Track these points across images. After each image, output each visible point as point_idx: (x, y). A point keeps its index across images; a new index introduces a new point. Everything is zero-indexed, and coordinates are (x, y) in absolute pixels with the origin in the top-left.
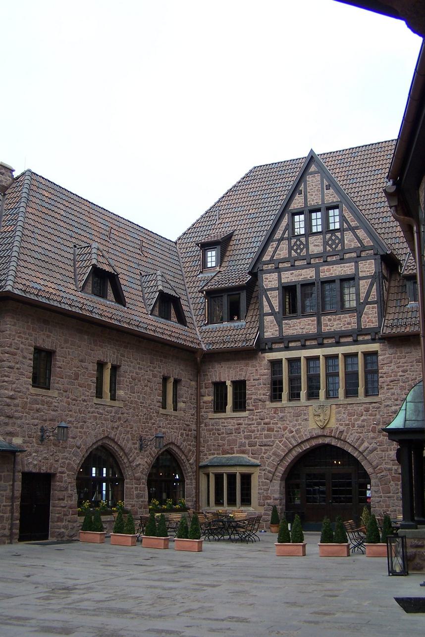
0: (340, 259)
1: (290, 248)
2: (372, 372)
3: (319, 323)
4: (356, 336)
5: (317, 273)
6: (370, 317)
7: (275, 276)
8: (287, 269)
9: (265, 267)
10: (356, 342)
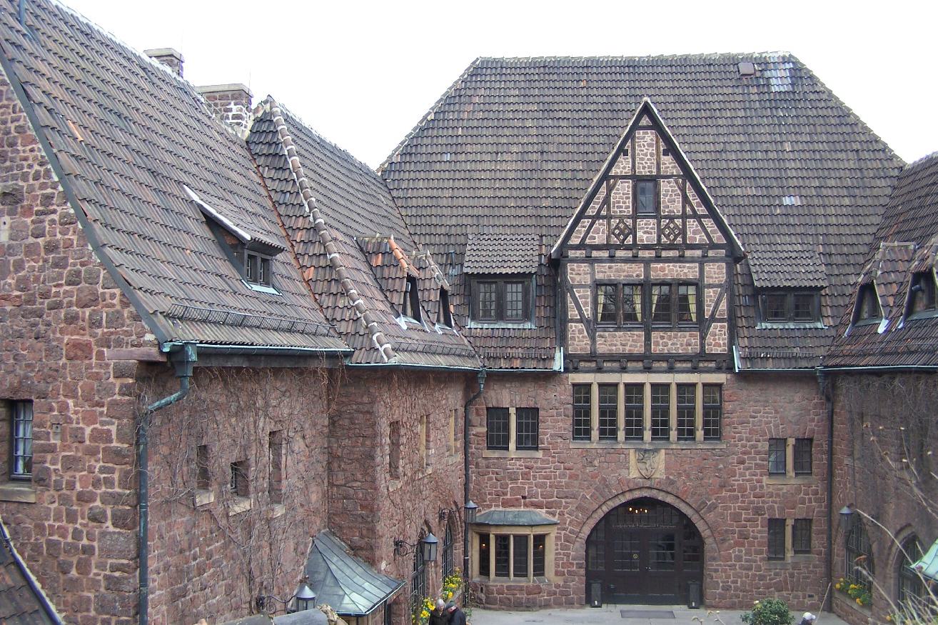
0: (680, 256)
2: (714, 414)
3: (648, 338)
4: (697, 361)
6: (717, 339)
7: (585, 267)
9: (572, 254)
10: (695, 370)
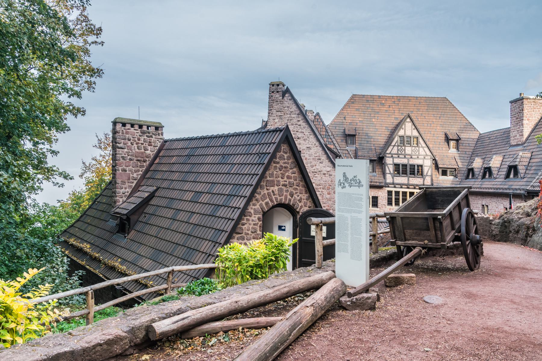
1: (398, 150)
3: (408, 180)
5: (408, 161)
7: (392, 159)
8: (396, 158)
9: (387, 155)
